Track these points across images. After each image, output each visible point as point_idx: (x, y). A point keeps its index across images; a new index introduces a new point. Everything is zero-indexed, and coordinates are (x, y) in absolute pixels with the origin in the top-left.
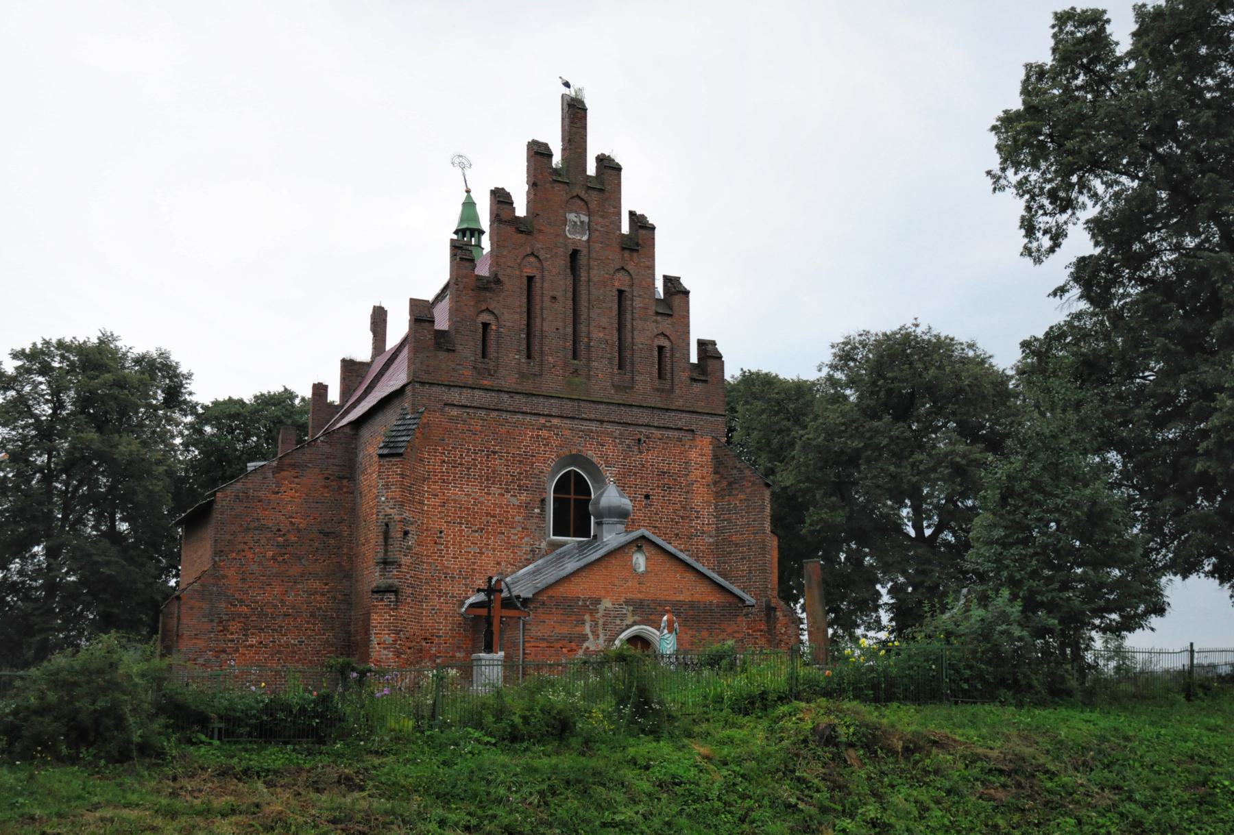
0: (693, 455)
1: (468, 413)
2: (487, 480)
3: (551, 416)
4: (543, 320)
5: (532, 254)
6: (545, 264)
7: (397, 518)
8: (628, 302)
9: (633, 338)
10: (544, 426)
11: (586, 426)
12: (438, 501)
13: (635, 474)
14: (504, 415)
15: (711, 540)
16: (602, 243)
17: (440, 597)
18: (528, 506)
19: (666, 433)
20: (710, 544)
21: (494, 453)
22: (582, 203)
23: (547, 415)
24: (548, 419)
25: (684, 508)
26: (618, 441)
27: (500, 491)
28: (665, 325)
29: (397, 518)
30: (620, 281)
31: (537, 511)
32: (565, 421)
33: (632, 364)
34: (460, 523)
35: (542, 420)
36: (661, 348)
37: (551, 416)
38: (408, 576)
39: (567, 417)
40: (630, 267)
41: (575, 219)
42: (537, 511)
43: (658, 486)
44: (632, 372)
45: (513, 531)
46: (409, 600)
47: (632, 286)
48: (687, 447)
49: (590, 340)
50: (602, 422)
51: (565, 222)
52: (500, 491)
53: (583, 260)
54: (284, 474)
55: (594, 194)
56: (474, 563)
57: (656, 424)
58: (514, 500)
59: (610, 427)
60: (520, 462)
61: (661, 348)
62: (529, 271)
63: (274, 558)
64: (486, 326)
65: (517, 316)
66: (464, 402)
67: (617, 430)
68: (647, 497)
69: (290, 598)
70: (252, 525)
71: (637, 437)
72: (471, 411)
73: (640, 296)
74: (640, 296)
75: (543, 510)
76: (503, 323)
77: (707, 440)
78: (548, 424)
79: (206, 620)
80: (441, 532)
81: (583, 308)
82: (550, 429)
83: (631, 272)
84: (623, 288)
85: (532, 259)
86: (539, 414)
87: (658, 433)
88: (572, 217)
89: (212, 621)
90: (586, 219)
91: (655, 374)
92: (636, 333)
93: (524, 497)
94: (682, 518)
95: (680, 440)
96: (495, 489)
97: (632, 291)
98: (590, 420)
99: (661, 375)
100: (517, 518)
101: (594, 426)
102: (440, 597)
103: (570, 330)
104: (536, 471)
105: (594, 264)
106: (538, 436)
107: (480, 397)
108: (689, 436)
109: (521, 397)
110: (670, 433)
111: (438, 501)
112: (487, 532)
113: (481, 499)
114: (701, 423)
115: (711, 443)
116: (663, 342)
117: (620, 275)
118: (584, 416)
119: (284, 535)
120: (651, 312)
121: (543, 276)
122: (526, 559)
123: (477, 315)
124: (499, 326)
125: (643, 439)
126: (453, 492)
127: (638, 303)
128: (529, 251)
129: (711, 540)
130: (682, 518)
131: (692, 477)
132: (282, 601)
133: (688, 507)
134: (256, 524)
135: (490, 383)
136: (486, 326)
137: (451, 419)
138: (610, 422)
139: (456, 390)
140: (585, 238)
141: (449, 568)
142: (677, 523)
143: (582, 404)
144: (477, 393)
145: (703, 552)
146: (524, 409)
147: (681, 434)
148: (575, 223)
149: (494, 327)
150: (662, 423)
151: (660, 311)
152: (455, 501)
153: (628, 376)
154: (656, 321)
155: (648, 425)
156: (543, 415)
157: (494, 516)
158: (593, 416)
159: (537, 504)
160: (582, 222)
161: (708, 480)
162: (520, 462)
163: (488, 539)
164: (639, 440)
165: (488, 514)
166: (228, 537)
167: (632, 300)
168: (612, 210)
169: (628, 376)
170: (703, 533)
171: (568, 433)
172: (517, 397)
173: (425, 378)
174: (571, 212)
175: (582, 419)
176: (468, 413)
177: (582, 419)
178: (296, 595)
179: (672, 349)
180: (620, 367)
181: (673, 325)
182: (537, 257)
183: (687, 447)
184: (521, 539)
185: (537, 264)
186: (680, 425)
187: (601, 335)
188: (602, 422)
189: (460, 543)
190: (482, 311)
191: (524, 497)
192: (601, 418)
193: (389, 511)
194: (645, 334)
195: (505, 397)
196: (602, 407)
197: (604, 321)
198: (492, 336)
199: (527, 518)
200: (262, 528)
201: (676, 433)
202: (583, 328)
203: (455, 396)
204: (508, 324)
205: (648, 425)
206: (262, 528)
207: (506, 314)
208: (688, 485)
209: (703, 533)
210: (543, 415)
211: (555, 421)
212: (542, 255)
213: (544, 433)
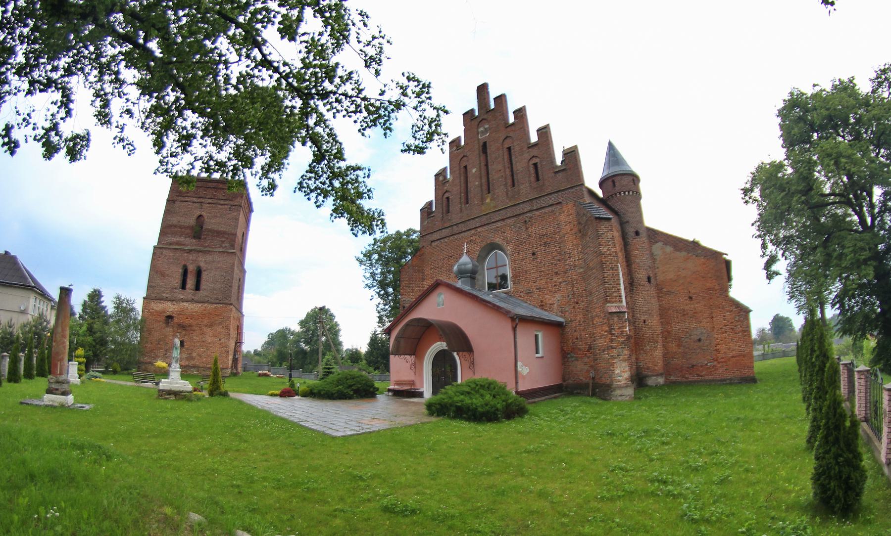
0: (562, 217)
3: (477, 227)
11: (494, 226)
13: (525, 242)
15: (582, 270)
19: (543, 211)
20: (581, 273)
23: (475, 228)
24: (476, 229)
25: (559, 253)
35: (473, 232)
37: (477, 227)
39: (484, 225)
48: (557, 214)
50: (503, 220)
57: (535, 208)
59: (508, 221)
61: (535, 165)
66: (439, 238)
77: (571, 205)
87: (537, 213)
91: (533, 178)
94: (559, 260)
95: (553, 211)
101: (499, 224)
103: (484, 180)
107: (445, 232)
108: (559, 207)
110: (546, 210)
114: (566, 195)
115: (574, 205)
116: (535, 161)
118: (493, 220)
125: (527, 220)
129: (582, 270)
130: (559, 260)
131: (564, 232)
133: (563, 253)
138: (507, 218)
142: (555, 265)
145: (577, 280)
147: (553, 208)
150: (539, 206)
154: (528, 152)
155: (530, 211)
158: (497, 219)
161: (576, 230)
164: (526, 221)
170: (575, 266)
172: (460, 225)
175: (493, 222)
182: (466, 156)
183: (557, 214)
186: (550, 202)
188: (503, 220)
190: (445, 193)
192: (501, 218)
194: (521, 164)
195: (455, 227)
197: (500, 167)
201: (550, 209)
205: (530, 211)
208: (561, 238)
209: (575, 266)
211: (479, 230)
213: (473, 238)
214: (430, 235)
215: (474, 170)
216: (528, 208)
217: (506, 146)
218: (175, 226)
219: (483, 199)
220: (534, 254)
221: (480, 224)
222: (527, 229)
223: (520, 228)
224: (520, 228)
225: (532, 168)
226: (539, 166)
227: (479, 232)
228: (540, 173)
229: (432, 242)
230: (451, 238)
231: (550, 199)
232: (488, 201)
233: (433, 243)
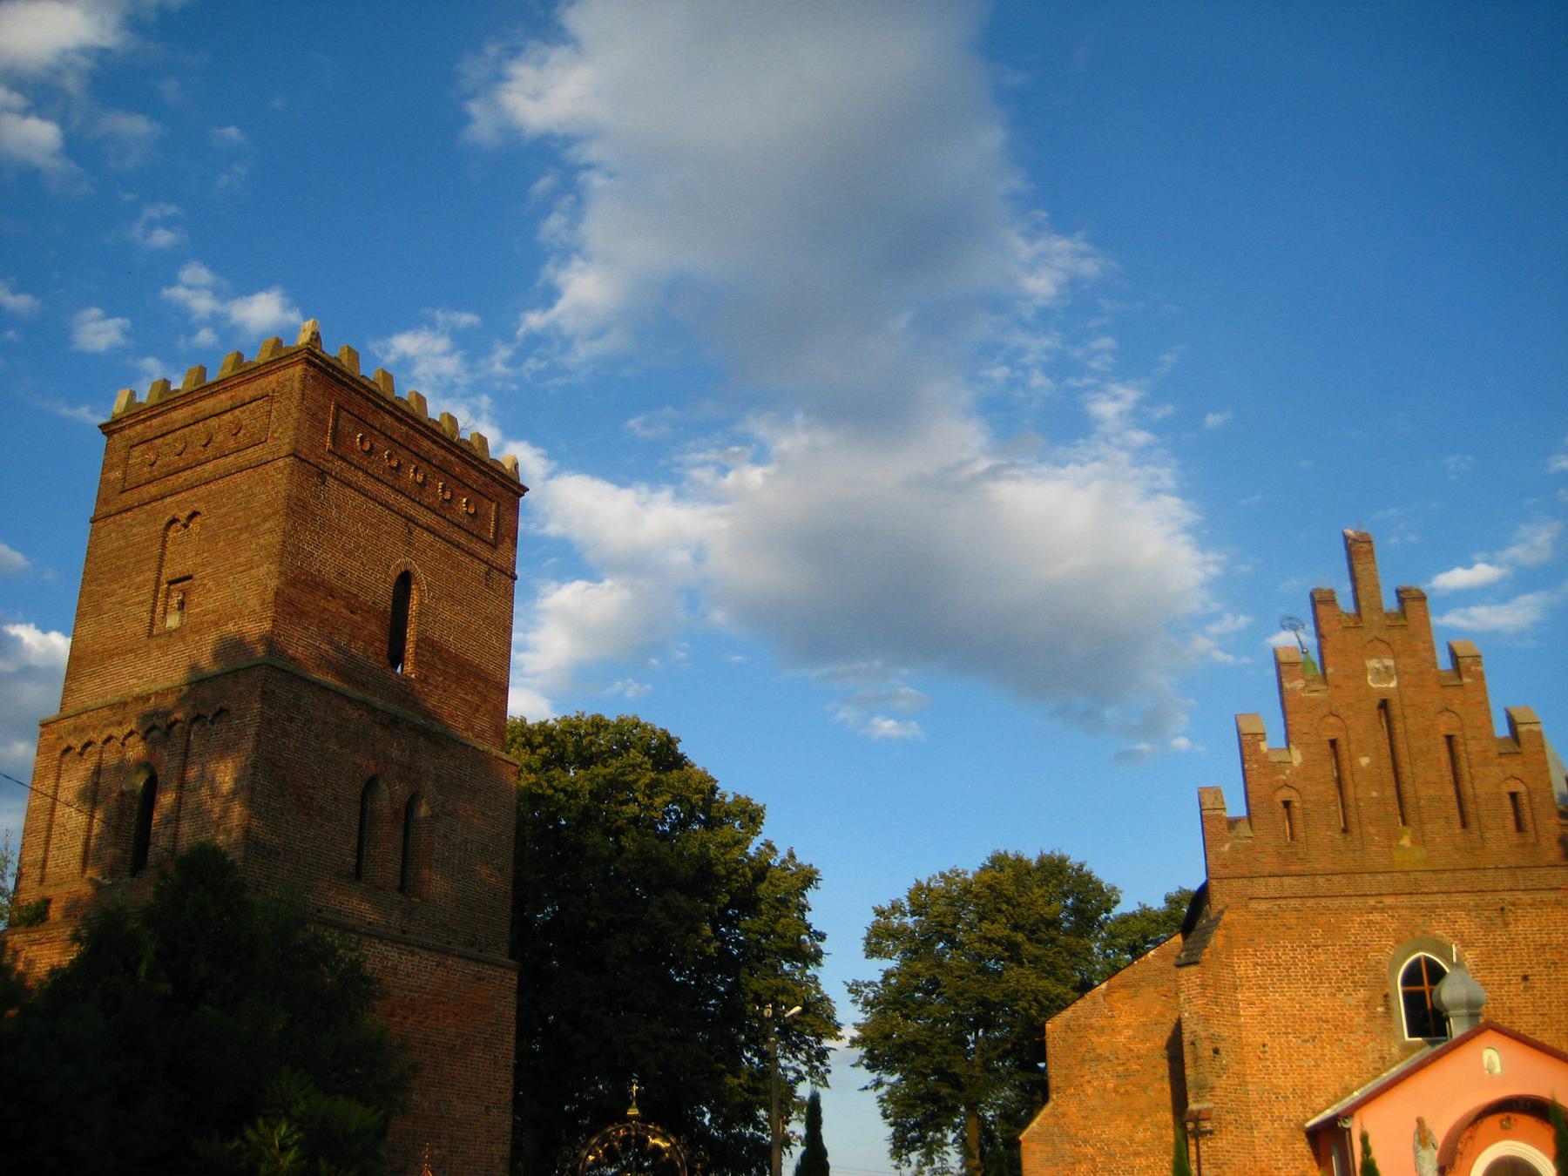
1: (1279, 906)
2: (1313, 979)
4: (1355, 786)
5: (1332, 714)
6: (1348, 722)
7: (1203, 1034)
8: (1461, 748)
9: (1474, 788)
10: (1374, 908)
11: (1426, 901)
12: (1256, 1010)
14: (1323, 902)
16: (1414, 686)
17: (1273, 1122)
18: (1368, 1004)
21: (1317, 947)
22: (1383, 647)
24: (1379, 899)
26: (1473, 914)
27: (1330, 990)
28: (1514, 767)
29: (1203, 1034)
30: (1445, 724)
31: (1380, 1009)
32: (1401, 899)
33: (1479, 818)
34: (1287, 1034)
35: (1372, 902)
36: (1514, 796)
37: (1382, 895)
38: (1226, 1100)
40: (1456, 707)
41: (1377, 665)
42: (1380, 1009)
43: (1538, 963)
44: (1480, 830)
45: (1352, 1036)
46: (1231, 1128)
47: (1462, 727)
49: (1418, 799)
51: (1365, 670)
52: (1330, 990)
53: (1396, 710)
54: (1115, 996)
55: (1396, 633)
56: (1309, 1078)
58: (1350, 999)
59: (1462, 899)
60: (1350, 954)
61: (1514, 796)
62: (1331, 735)
63: (1115, 1091)
64: (1287, 804)
65: (1322, 788)
66: (1272, 893)
67: (1470, 900)
68: (1525, 978)
69: (1139, 1136)
70: (1087, 1057)
71: (1498, 907)
72: (1282, 902)
73: (1474, 738)
74: (1474, 738)
75: (1388, 1008)
76: (1307, 798)
78: (1380, 905)
79: (1049, 1163)
80: (1264, 1046)
81: (1403, 765)
82: (1382, 910)
83: (1458, 711)
84: (1450, 733)
85: (1332, 720)
86: (1366, 895)
88: (1372, 664)
89: (1057, 1165)
90: (1390, 663)
92: (1476, 782)
93: (1362, 993)
96: (1324, 989)
97: (1464, 736)
98: (1433, 893)
99: (1520, 826)
100: (1357, 1020)
101: (1439, 899)
102: (1273, 1122)
103: (1391, 792)
104: (1373, 963)
105: (1408, 711)
106: (1369, 921)
109: (1339, 878)
111: (1256, 1010)
112: (1322, 1041)
113: (1308, 1003)
117: (1445, 717)
119: (1124, 1064)
120: (1493, 753)
121: (1348, 736)
122: (1375, 1069)
123: (1274, 792)
124: (1304, 802)
126: (1273, 998)
127: (1473, 747)
128: (1326, 711)
132: (1132, 1141)
134: (1092, 1055)
135: (1301, 868)
136: (1287, 804)
137: (1259, 915)
139: (1262, 880)
140: (1393, 684)
141: (1277, 1086)
143: (1418, 875)
144: (1287, 880)
146: (1347, 892)
148: (1378, 669)
149: (1297, 804)
151: (1503, 751)
152: (1276, 1008)
153: (1476, 835)
154: (1500, 764)
156: (1372, 895)
157: (1327, 1021)
158: (1435, 889)
159: (1380, 1000)
160: (1387, 668)
162: (1350, 954)
163: (1323, 1048)
164: (1502, 909)
165: (1319, 1019)
166: (1065, 1071)
167: (1466, 745)
168: (1421, 645)
169: (1476, 835)
171: (1406, 913)
172: (1335, 879)
173: (1223, 873)
174: (1371, 657)
175: (1422, 893)
176: (1279, 906)
177: (1422, 893)
178: (1145, 1130)
179: (1529, 794)
180: (1464, 824)
181: (1524, 764)
184: (1365, 1044)
185: (1340, 724)
186: (1555, 884)
187: (1431, 792)
189: (1290, 1055)
191: (1362, 993)
192: (1443, 888)
193: (1194, 1027)
195: (1321, 880)
196: (1446, 875)
198: (1297, 814)
199: (1369, 1019)
200: (1099, 1059)
202: (1408, 789)
203: (1260, 887)
204: (1313, 798)
206: (1099, 1059)
207: (1309, 787)
210: (1372, 895)
211: (1388, 901)
212: (1343, 712)
213: (1376, 917)
214: (1245, 881)
215: (1364, 761)
216: (1507, 884)
217: (1443, 730)
218: (331, 593)
219: (1393, 836)
220: (1525, 978)
221: (1391, 890)
222: (1507, 924)
223: (1489, 918)
224: (1489, 918)
225: (1507, 803)
226: (1524, 799)
227: (1391, 908)
228: (1527, 816)
229: (1250, 899)
230: (1311, 902)
231: (1555, 877)
232: (1405, 841)
233: (1253, 904)
